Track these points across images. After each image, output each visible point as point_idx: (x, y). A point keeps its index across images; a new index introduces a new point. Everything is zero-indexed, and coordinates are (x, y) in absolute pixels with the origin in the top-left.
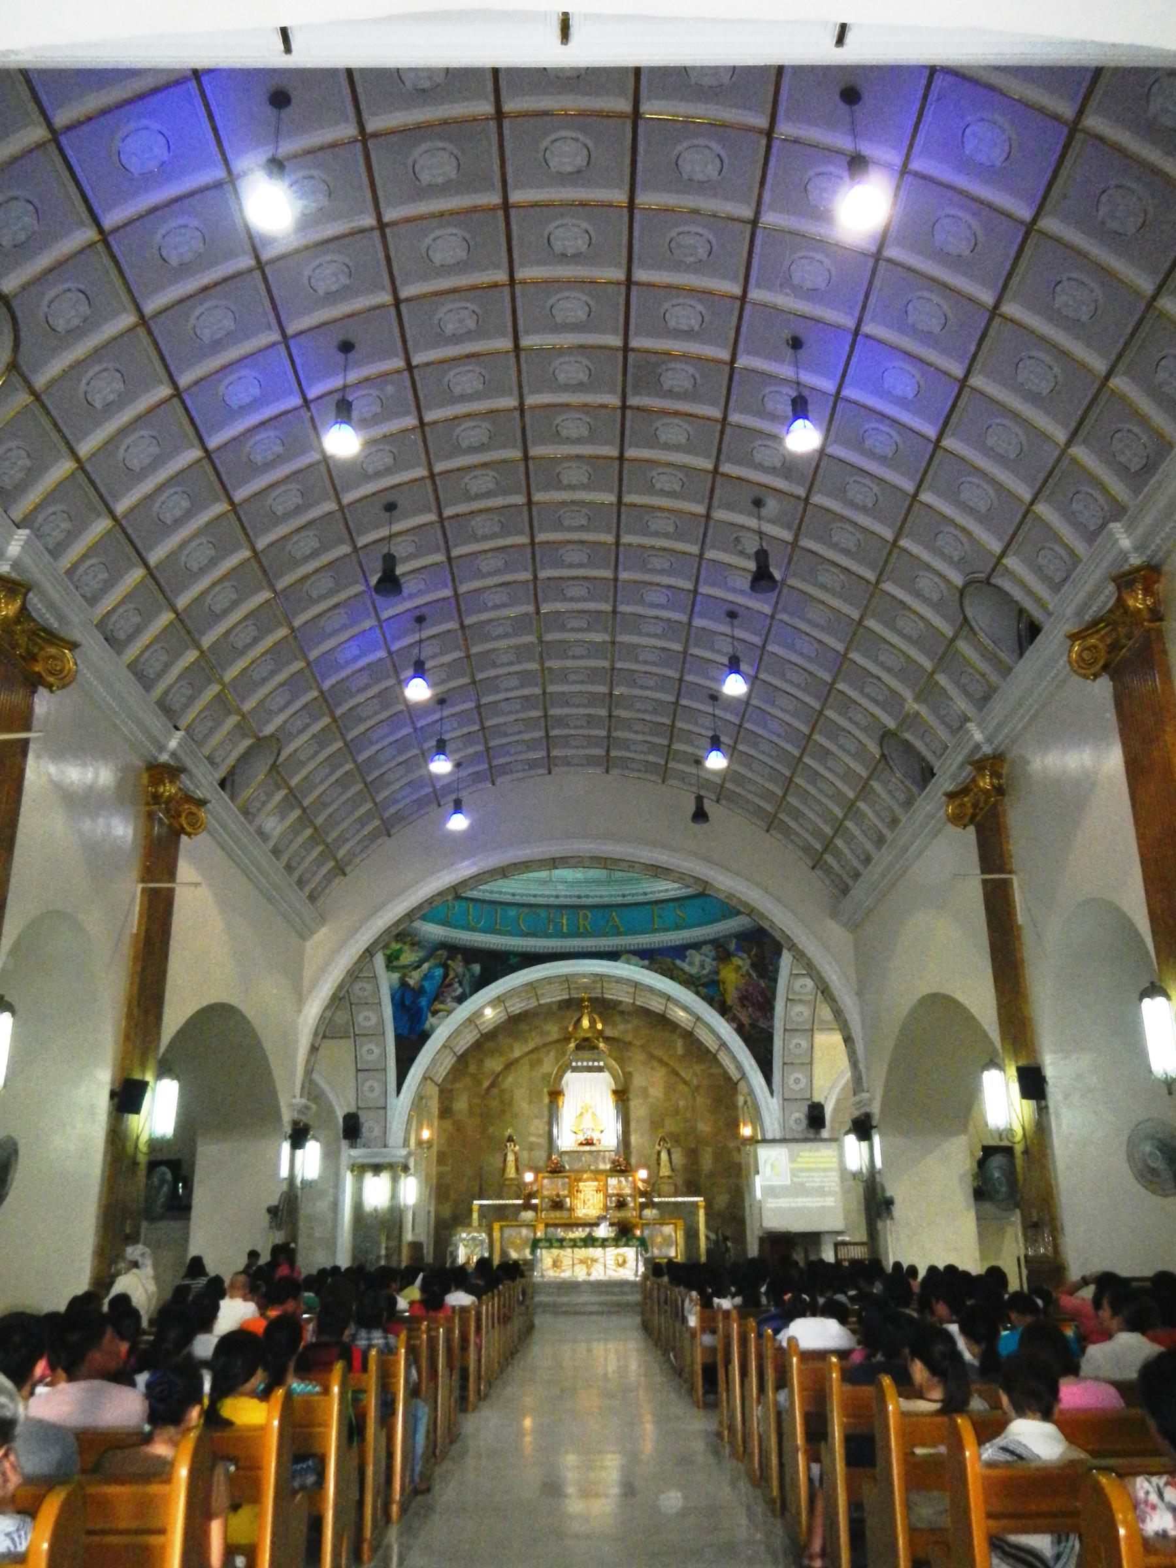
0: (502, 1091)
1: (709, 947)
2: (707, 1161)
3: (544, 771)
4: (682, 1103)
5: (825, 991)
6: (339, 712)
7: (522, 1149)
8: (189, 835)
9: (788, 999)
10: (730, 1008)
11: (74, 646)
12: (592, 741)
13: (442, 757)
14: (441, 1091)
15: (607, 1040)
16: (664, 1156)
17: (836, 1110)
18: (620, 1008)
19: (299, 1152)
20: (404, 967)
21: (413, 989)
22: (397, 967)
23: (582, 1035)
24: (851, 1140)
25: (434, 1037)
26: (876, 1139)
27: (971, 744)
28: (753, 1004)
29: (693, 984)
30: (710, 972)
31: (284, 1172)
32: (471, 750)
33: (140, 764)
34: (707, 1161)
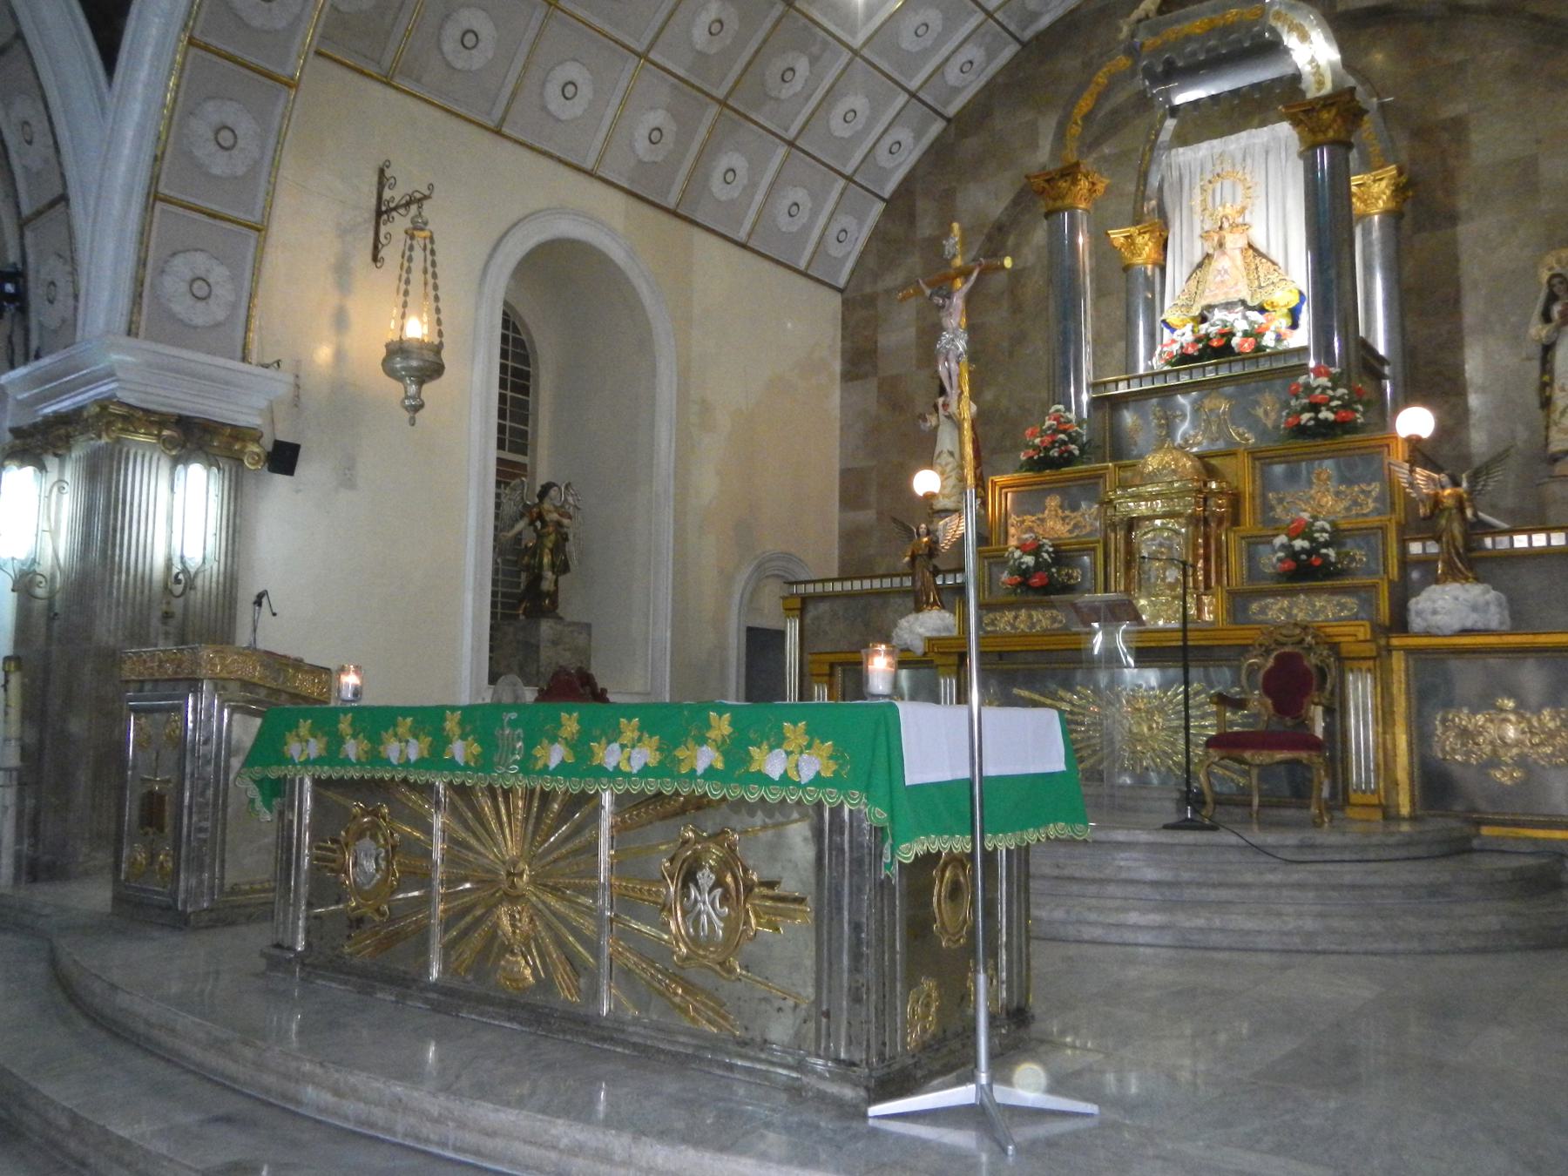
14: (845, 303)
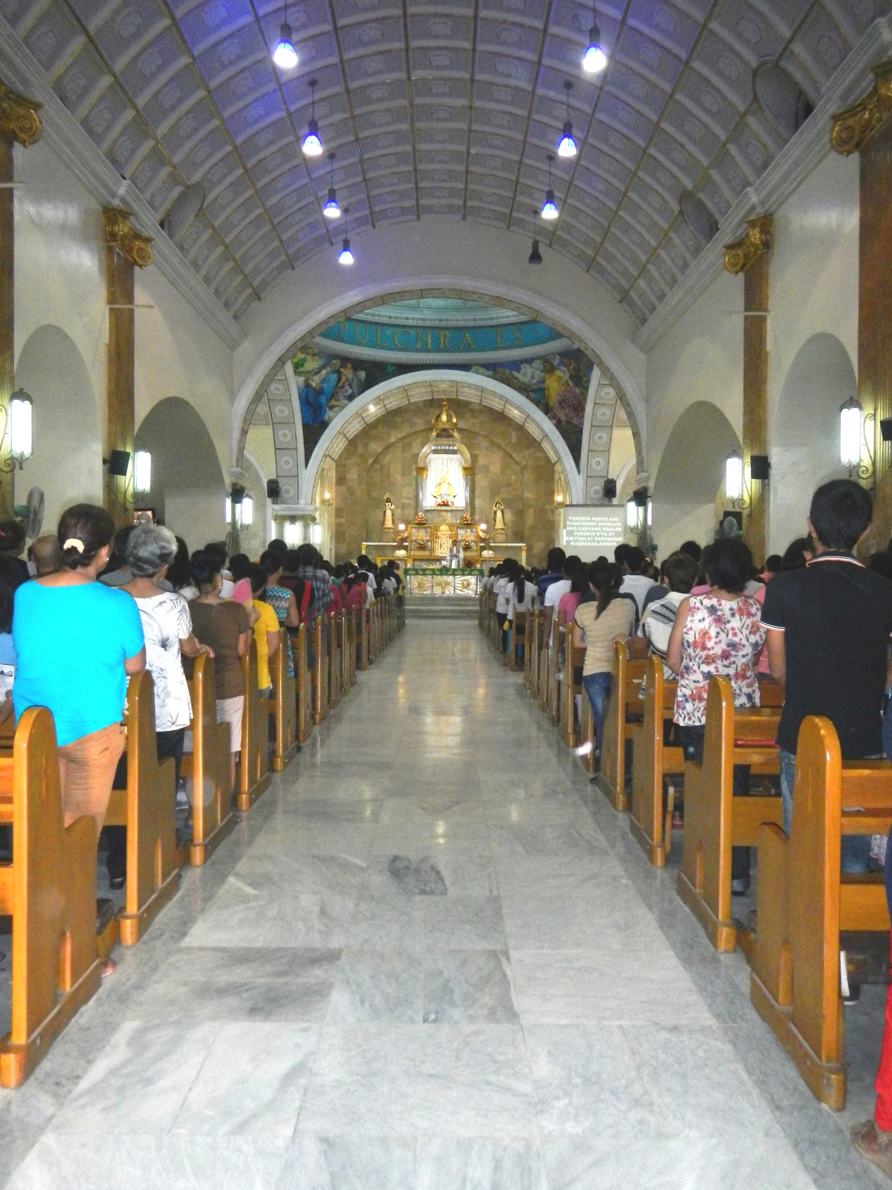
0: (382, 467)
1: (538, 362)
2: (530, 519)
3: (415, 217)
4: (513, 478)
5: (622, 397)
6: (250, 164)
7: (397, 507)
8: (141, 266)
9: (596, 404)
10: (552, 409)
11: (37, 106)
12: (452, 193)
13: (333, 204)
14: (338, 465)
15: (460, 430)
16: (499, 514)
17: (624, 486)
18: (471, 407)
19: (238, 506)
20: (308, 372)
21: (315, 389)
22: (302, 372)
23: (442, 426)
24: (632, 505)
25: (330, 426)
26: (650, 505)
27: (748, 207)
28: (569, 406)
29: (525, 390)
30: (538, 382)
31: (229, 519)
32: (354, 199)
33: (100, 208)
34: (530, 519)
